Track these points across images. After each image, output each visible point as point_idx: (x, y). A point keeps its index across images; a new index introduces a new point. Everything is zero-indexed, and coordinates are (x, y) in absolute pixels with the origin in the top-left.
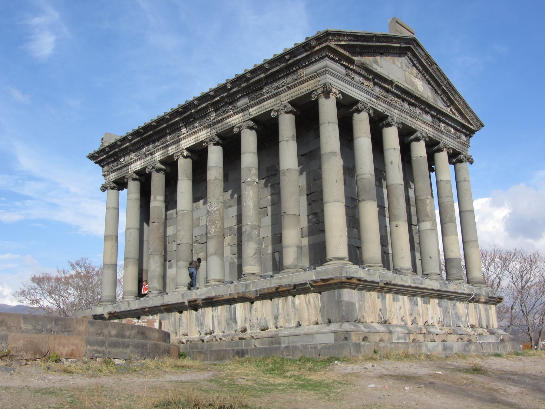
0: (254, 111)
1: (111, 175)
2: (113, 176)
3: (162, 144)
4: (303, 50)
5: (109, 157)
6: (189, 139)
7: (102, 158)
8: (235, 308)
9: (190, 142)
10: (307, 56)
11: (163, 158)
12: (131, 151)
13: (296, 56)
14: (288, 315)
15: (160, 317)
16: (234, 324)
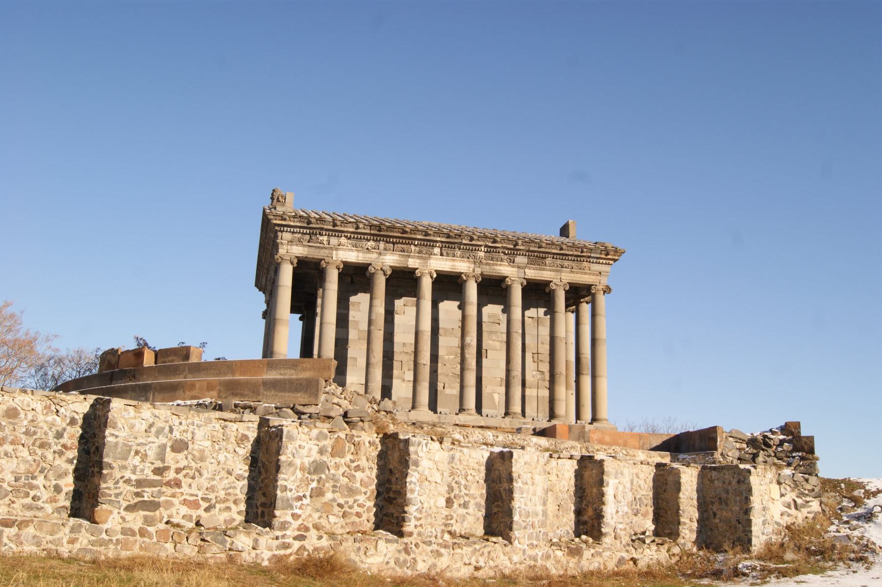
1: (294, 247)
2: (299, 251)
6: (443, 263)
7: (292, 224)
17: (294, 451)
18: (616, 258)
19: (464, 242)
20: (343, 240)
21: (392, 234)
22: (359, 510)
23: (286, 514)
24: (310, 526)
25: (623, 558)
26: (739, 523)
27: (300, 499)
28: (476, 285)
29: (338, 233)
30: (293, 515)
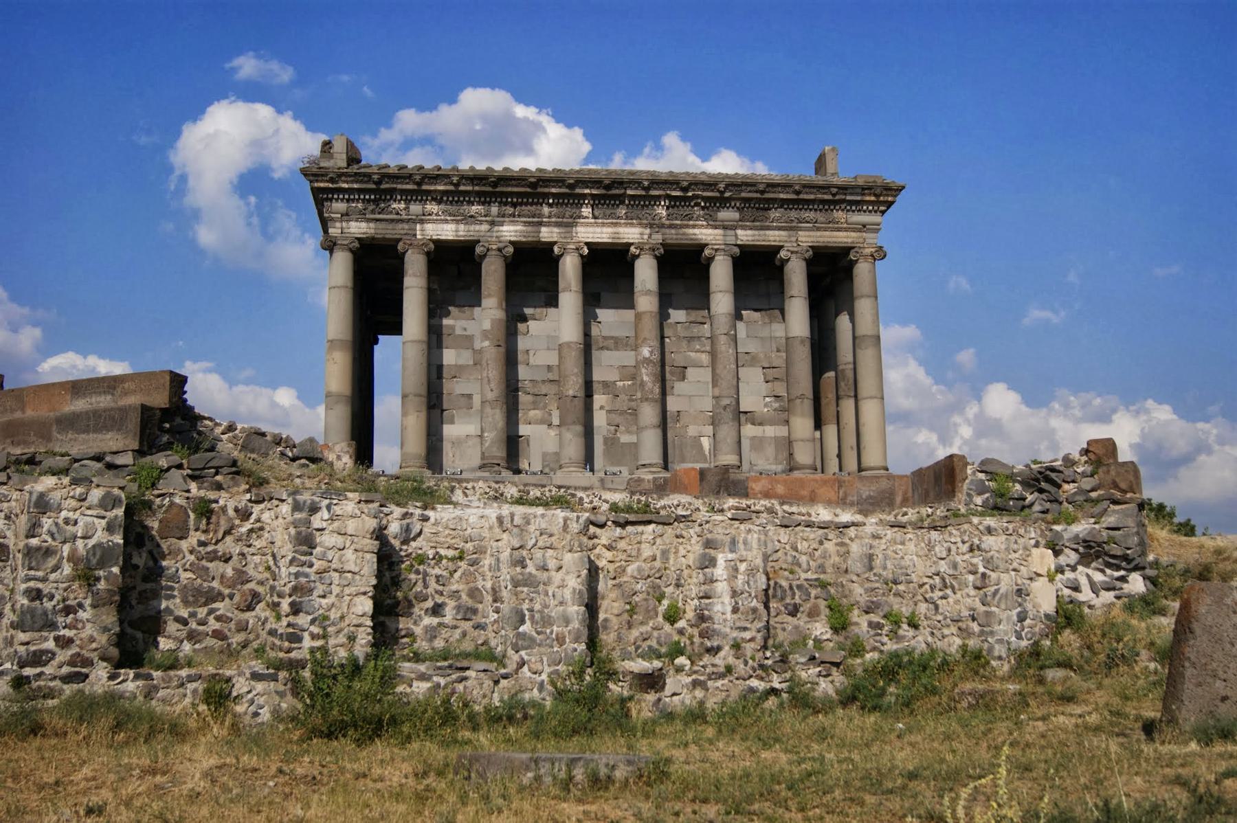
0: (746, 236)
1: (353, 224)
2: (359, 228)
5: (360, 191)
6: (598, 230)
7: (345, 186)
10: (857, 203)
12: (433, 199)
17: (54, 529)
19: (629, 192)
21: (509, 189)
22: (217, 626)
23: (46, 639)
24: (95, 656)
25: (752, 690)
26: (974, 619)
27: (68, 610)
28: (654, 262)
29: (419, 195)
30: (57, 639)
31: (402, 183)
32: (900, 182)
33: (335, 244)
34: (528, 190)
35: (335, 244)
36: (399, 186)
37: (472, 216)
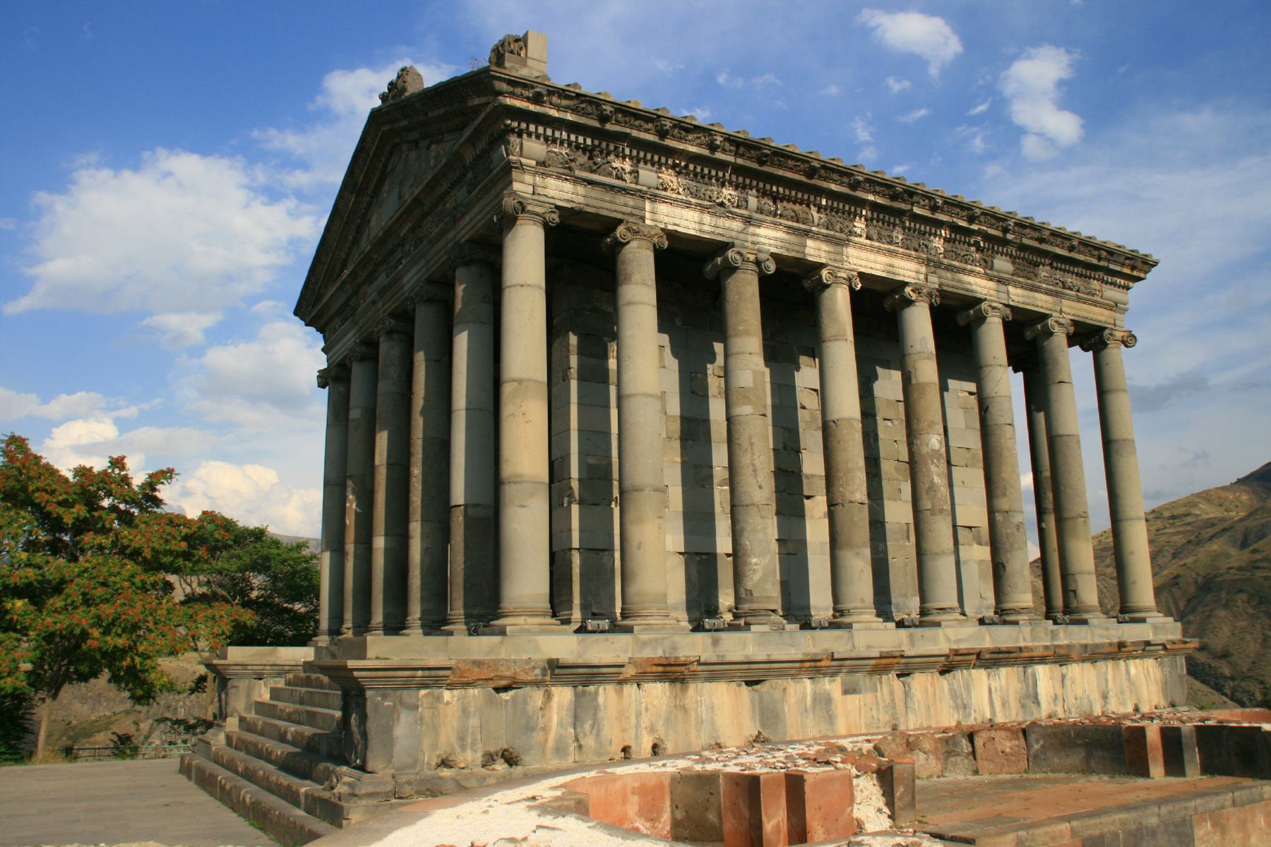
0: (1018, 296)
1: (551, 182)
2: (561, 192)
3: (792, 219)
4: (1122, 259)
5: (573, 127)
6: (872, 256)
7: (554, 113)
8: (1034, 675)
9: (872, 265)
11: (785, 253)
12: (674, 167)
13: (1109, 261)
14: (1122, 693)
15: (843, 684)
16: (1034, 707)
18: (1142, 275)
19: (917, 210)
20: (668, 177)
21: (781, 172)
31: (639, 128)
32: (1155, 258)
33: (523, 210)
34: (803, 179)
35: (523, 210)
36: (635, 133)
37: (722, 204)
